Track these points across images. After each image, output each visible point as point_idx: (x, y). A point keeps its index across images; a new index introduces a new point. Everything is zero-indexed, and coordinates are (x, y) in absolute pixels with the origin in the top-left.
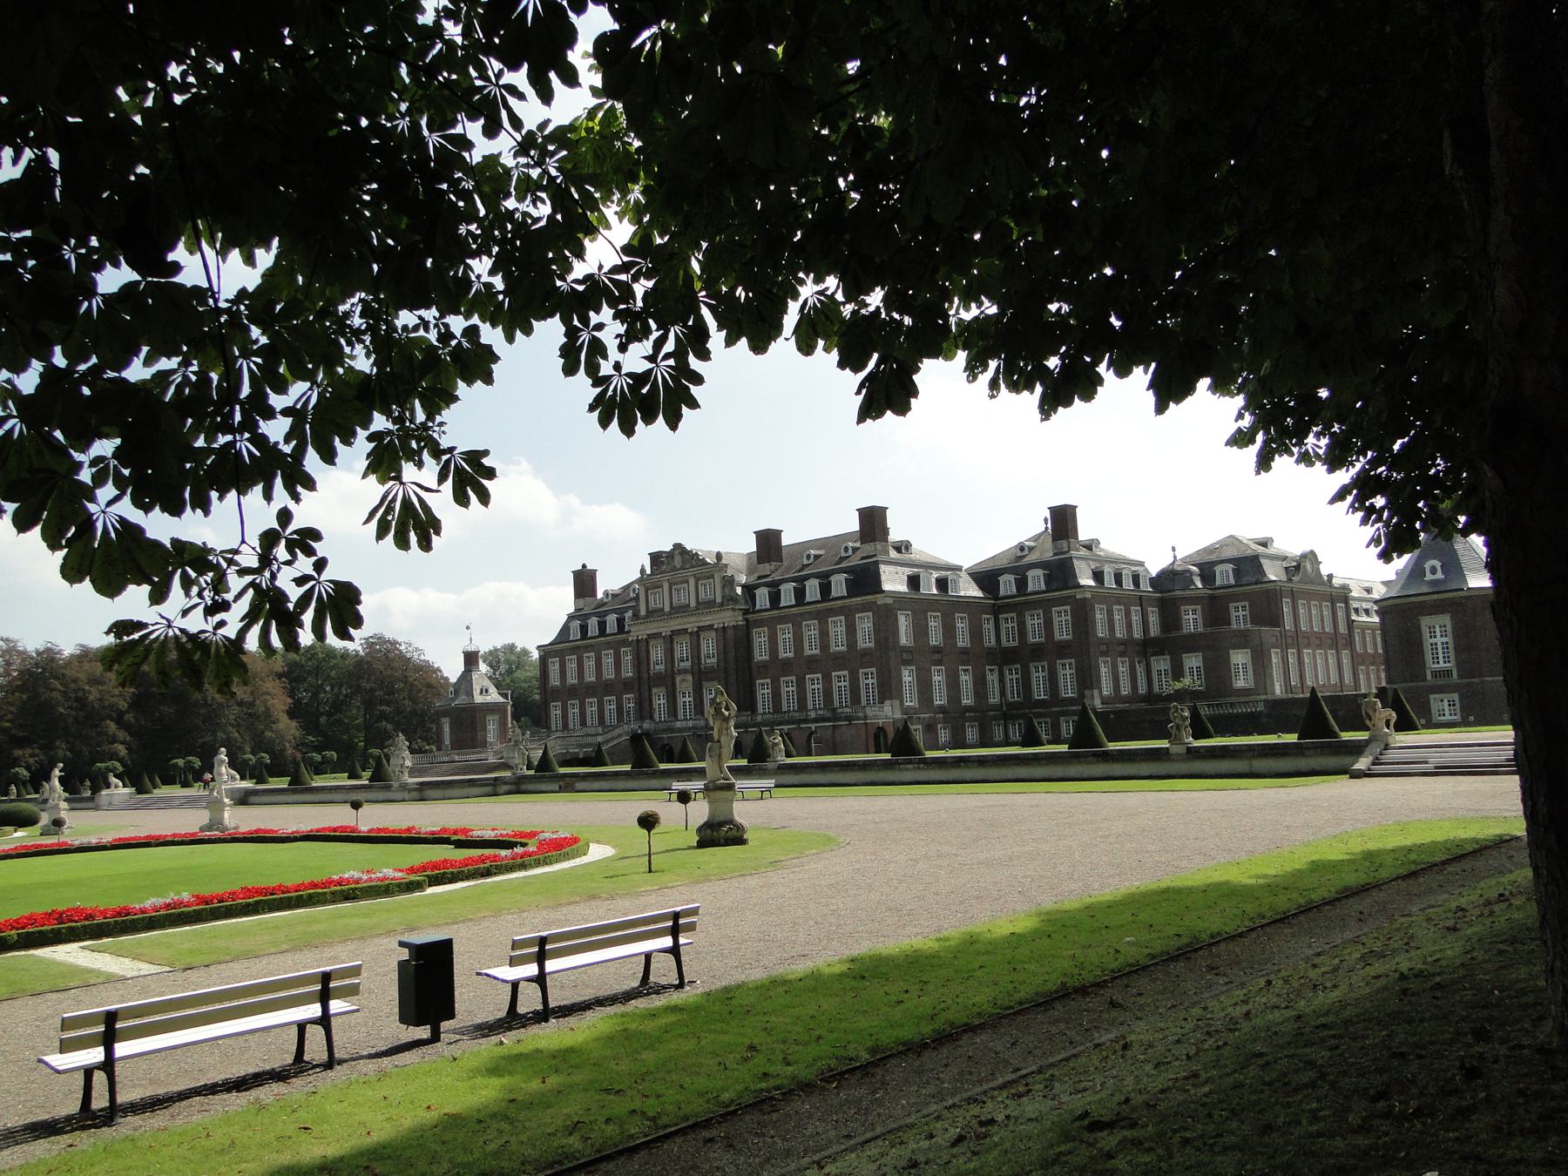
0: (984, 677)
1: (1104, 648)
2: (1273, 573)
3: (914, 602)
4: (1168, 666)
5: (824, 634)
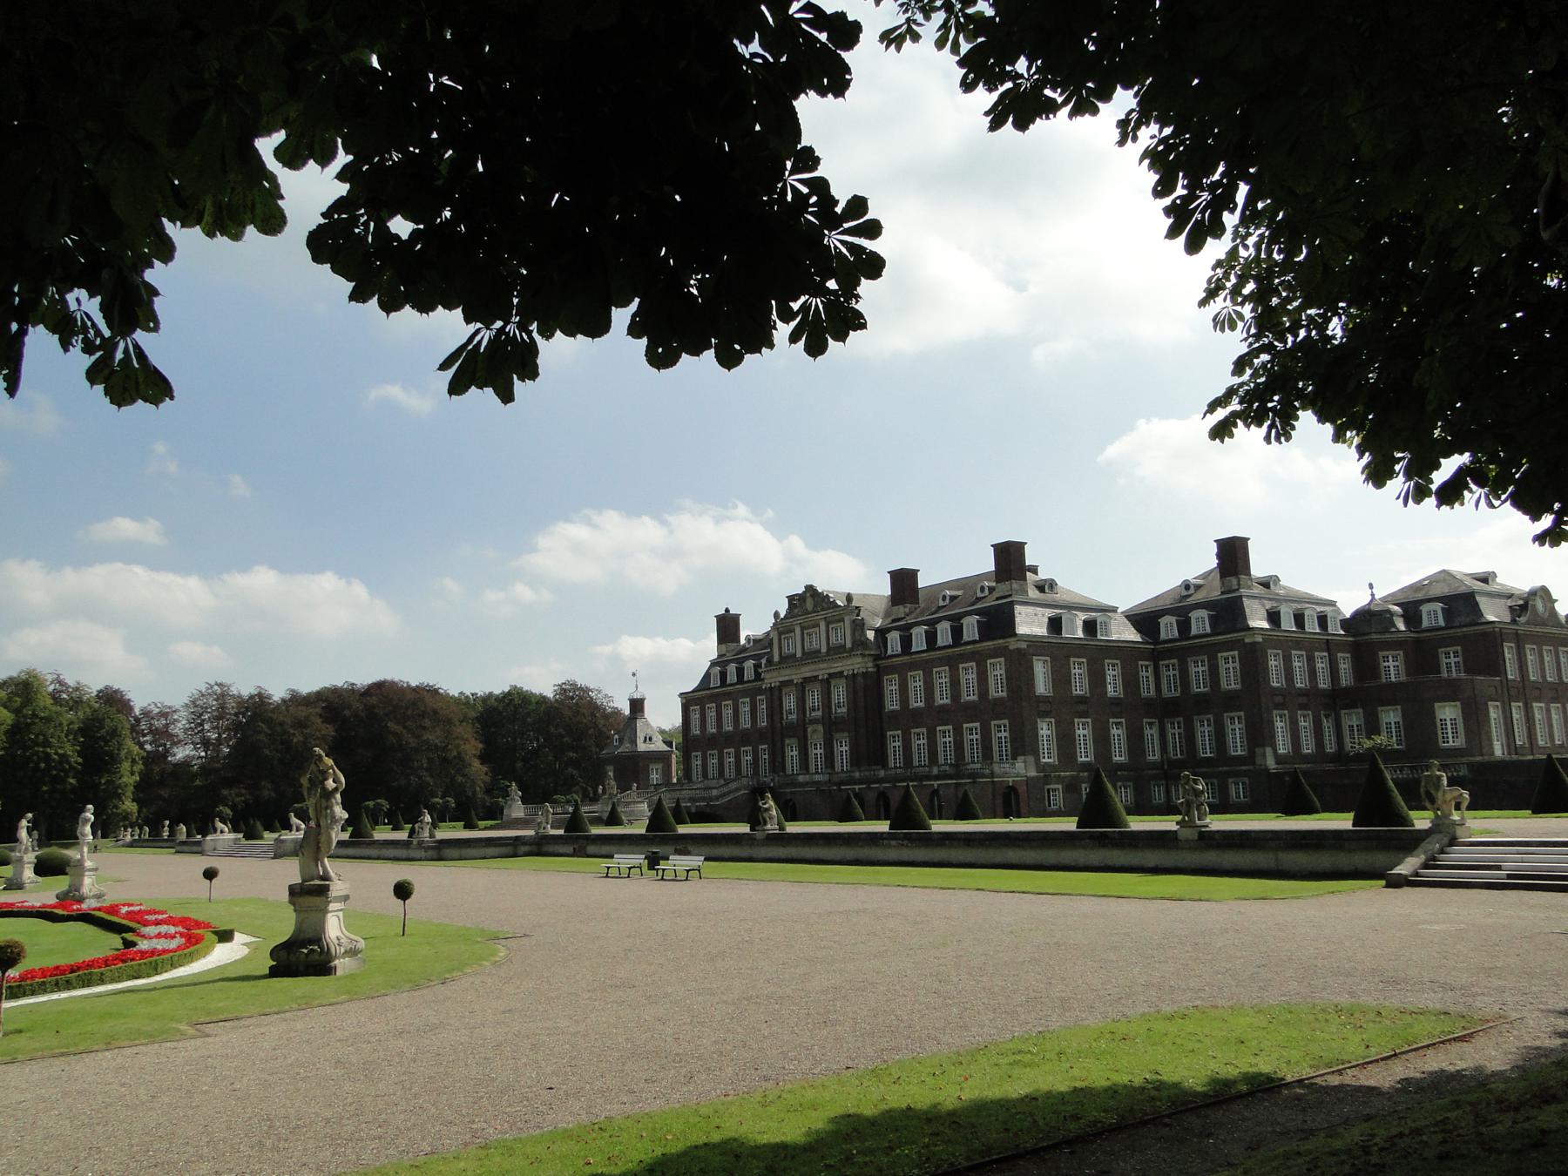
0: (1141, 736)
1: (1279, 699)
2: (1493, 613)
3: (1055, 647)
5: (955, 683)
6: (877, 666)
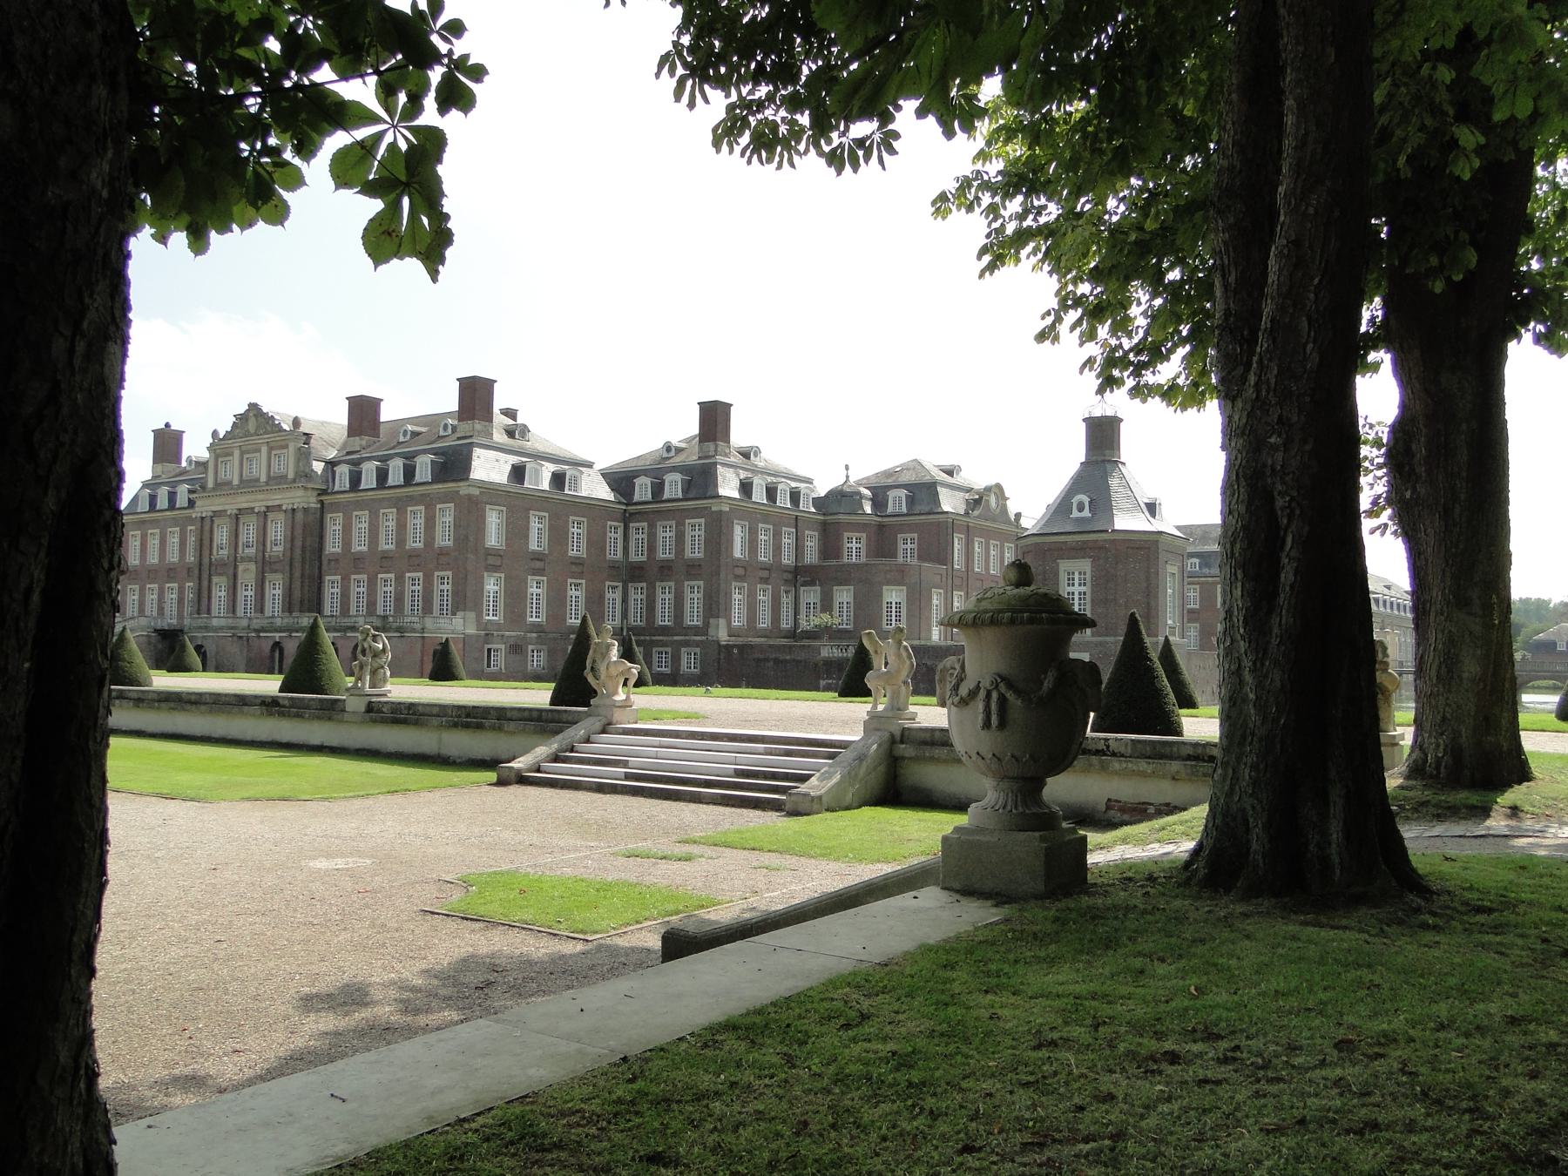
0: (602, 597)
1: (740, 571)
2: (950, 503)
3: (514, 496)
5: (401, 526)
6: (322, 502)
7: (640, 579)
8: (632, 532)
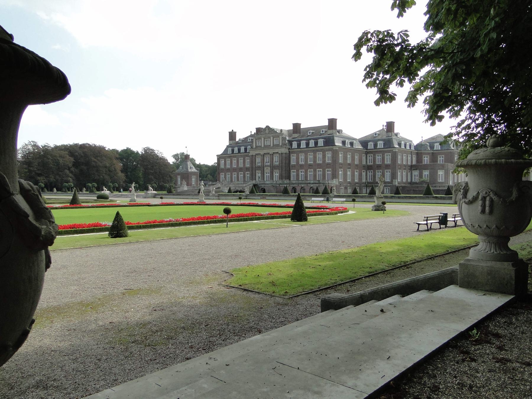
4: (428, 174)
5: (315, 157)
7: (370, 169)
8: (368, 157)
